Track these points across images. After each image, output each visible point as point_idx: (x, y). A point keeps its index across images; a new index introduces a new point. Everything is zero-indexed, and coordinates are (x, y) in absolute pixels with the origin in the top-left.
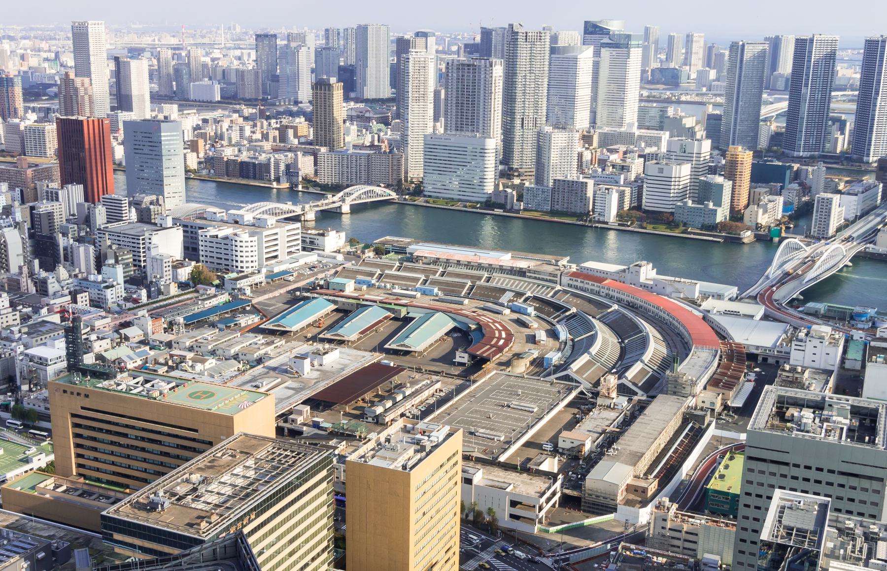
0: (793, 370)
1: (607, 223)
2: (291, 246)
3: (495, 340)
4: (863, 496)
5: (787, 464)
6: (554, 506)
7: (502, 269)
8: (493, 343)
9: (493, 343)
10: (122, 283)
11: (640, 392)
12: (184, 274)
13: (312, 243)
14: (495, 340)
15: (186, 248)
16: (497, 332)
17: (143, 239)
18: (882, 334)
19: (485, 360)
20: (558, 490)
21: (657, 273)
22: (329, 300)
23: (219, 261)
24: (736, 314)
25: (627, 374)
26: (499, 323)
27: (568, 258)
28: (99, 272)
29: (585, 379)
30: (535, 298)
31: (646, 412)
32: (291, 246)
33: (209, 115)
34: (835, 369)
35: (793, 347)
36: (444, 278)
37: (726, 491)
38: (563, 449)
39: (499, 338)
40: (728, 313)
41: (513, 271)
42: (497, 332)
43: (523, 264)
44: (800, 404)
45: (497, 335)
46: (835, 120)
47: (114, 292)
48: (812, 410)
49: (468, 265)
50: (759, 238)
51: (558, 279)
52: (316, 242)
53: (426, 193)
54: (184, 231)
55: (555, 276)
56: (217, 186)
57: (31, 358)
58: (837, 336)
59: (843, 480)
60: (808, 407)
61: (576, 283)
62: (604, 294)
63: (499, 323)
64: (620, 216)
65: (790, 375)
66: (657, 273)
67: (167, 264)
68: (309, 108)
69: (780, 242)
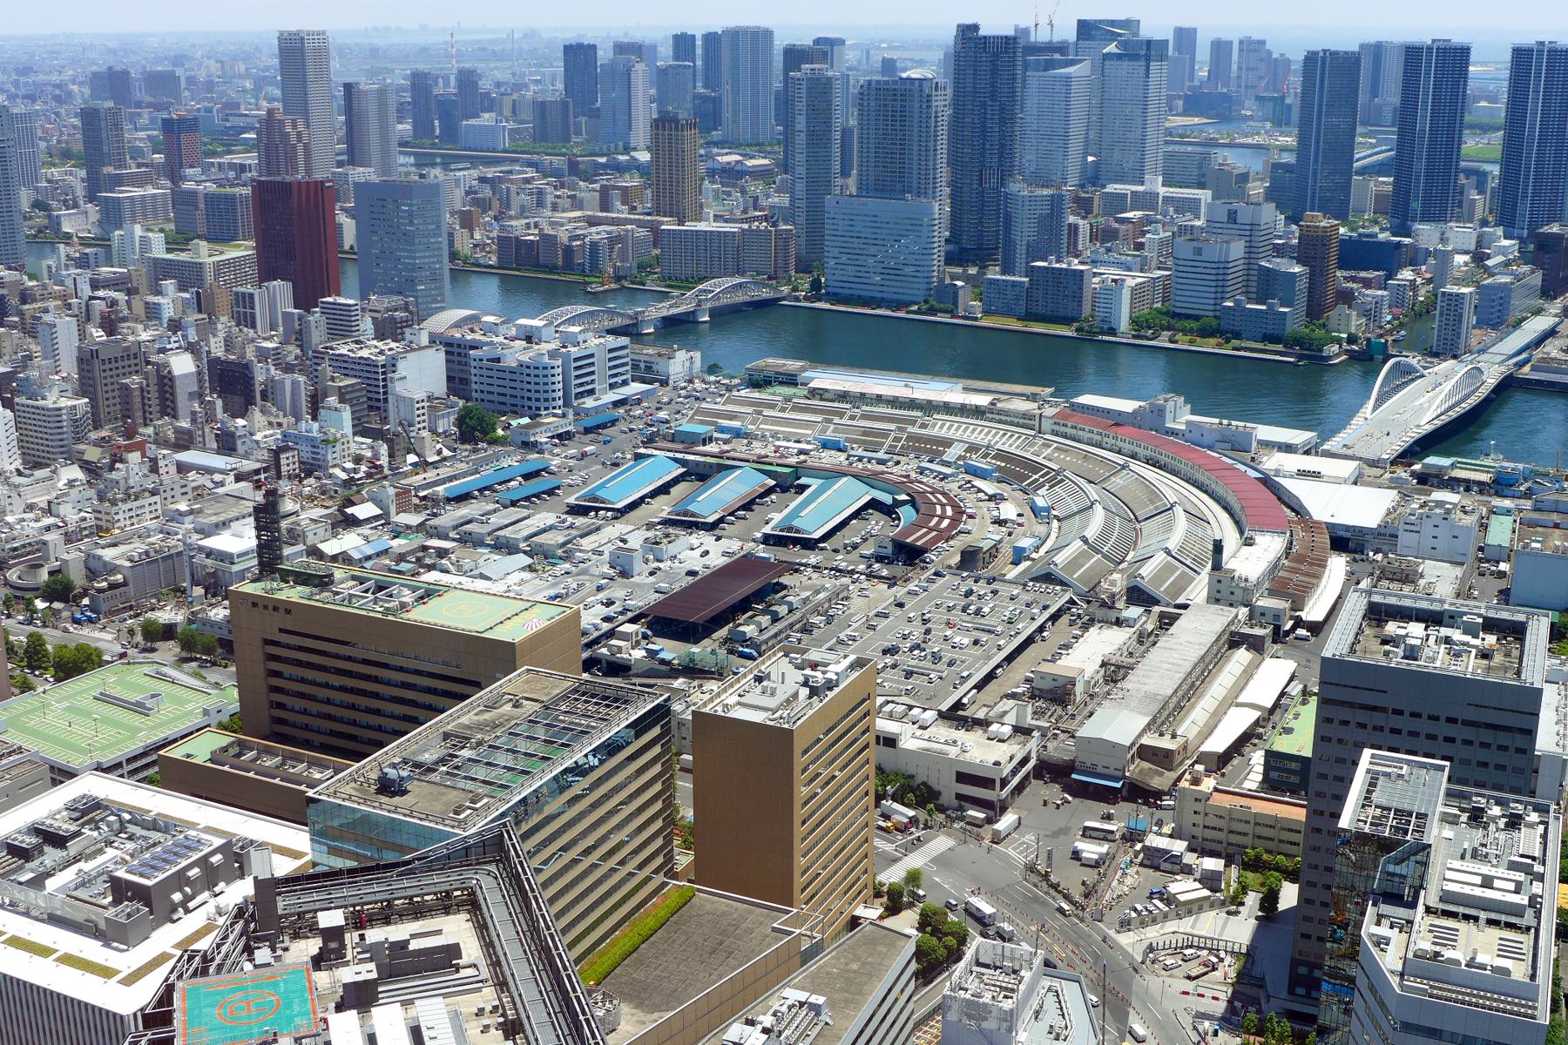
2: (615, 375)
4: (1501, 758)
5: (1384, 710)
8: (932, 524)
9: (932, 524)
13: (649, 368)
15: (450, 379)
20: (1034, 755)
21: (1193, 412)
22: (676, 460)
23: (502, 399)
24: (1316, 475)
26: (944, 494)
28: (314, 418)
31: (1172, 630)
32: (615, 375)
33: (490, 172)
36: (855, 423)
39: (942, 518)
40: (1303, 474)
43: (983, 400)
44: (1405, 615)
45: (939, 512)
46: (1469, 172)
48: (1423, 625)
49: (894, 402)
50: (1354, 357)
54: (447, 353)
55: (1032, 417)
56: (502, 282)
57: (210, 553)
59: (1469, 733)
60: (1418, 620)
64: (1136, 323)
68: (644, 156)
69: (1385, 362)
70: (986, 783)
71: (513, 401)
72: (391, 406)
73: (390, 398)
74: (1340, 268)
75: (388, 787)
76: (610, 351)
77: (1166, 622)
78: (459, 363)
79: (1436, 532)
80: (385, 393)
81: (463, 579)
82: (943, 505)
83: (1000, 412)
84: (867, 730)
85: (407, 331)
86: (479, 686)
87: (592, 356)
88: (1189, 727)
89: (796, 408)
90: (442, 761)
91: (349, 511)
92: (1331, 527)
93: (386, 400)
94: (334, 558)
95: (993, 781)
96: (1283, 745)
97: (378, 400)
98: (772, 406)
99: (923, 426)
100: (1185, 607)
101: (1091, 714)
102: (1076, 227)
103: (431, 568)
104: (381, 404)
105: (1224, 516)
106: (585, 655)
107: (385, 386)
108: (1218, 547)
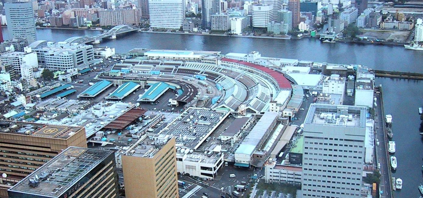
0: (324, 95)
1: (237, 35)
2: (89, 57)
3: (189, 93)
6: (221, 167)
7: (190, 60)
8: (188, 94)
9: (188, 94)
10: (10, 80)
11: (257, 112)
12: (39, 74)
13: (99, 54)
14: (189, 93)
15: (39, 62)
16: (189, 89)
17: (18, 59)
18: (361, 76)
19: (185, 103)
20: (223, 159)
21: (261, 56)
25: (250, 104)
27: (220, 52)
29: (231, 108)
30: (205, 73)
31: (260, 120)
32: (89, 57)
34: (343, 93)
35: (324, 85)
36: (163, 66)
37: (298, 153)
38: (224, 141)
41: (195, 60)
42: (189, 89)
44: (325, 111)
45: (189, 91)
47: (6, 86)
49: (174, 59)
51: (216, 62)
52: (101, 54)
53: (151, 27)
54: (38, 54)
55: (215, 61)
58: (342, 79)
61: (224, 63)
62: (238, 68)
63: (191, 85)
65: (323, 98)
66: (261, 56)
67: (31, 70)
70: (210, 169)
71: (59, 67)
72: (22, 71)
73: (21, 69)
74: (301, 11)
75: (33, 185)
76: (87, 50)
77: (258, 118)
78: (42, 57)
79: (333, 86)
80: (20, 67)
81: (48, 122)
82: (190, 88)
83: (205, 60)
84: (173, 157)
85: (25, 48)
86: (57, 153)
87: (82, 51)
88: (267, 149)
89: (145, 63)
90: (47, 177)
91: (12, 104)
92: (302, 86)
93: (20, 70)
94: (8, 118)
95: (212, 168)
96: (294, 150)
97: (18, 70)
98: (137, 63)
99: (183, 65)
100: (263, 113)
101: (239, 146)
102: (223, 3)
103: (39, 119)
104: (19, 71)
105: (272, 86)
106: (88, 142)
107: (19, 65)
108: (272, 95)
